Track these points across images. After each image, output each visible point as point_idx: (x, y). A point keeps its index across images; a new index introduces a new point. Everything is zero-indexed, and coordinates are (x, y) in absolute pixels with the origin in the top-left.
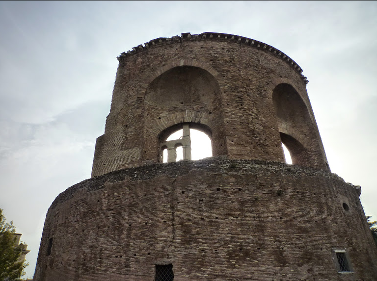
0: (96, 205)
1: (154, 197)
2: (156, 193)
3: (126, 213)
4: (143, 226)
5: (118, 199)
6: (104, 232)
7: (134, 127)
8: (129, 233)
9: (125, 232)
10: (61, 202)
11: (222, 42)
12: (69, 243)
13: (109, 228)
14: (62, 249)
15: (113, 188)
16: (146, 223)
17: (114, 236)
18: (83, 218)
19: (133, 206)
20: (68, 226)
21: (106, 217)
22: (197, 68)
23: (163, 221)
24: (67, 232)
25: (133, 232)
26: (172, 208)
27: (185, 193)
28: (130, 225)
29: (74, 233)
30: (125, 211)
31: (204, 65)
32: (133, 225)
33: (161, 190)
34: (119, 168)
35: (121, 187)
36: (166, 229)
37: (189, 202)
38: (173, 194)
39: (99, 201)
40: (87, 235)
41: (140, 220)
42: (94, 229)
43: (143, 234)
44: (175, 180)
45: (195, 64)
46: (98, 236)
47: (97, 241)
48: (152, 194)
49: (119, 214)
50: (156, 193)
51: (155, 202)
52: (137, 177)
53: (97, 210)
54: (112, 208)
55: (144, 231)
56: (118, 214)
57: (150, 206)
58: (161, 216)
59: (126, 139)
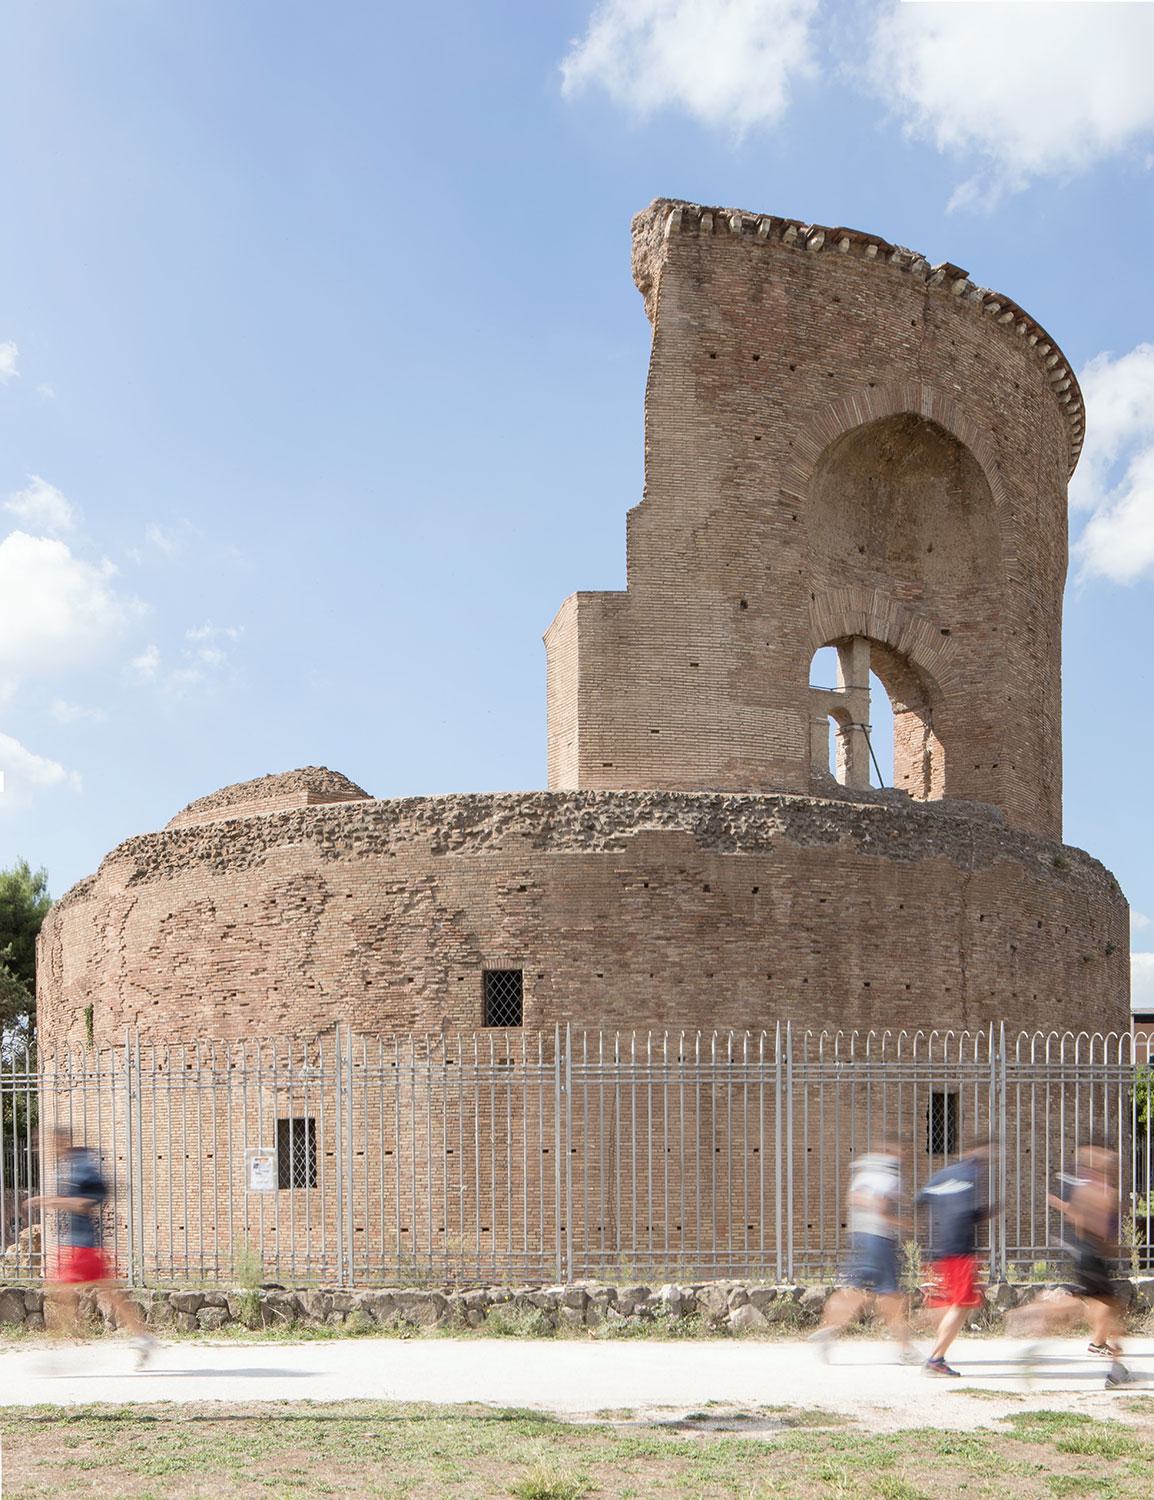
0: (750, 901)
1: (924, 919)
2: (928, 907)
3: (854, 948)
4: (900, 992)
5: (823, 901)
6: (791, 989)
7: (775, 622)
8: (866, 1009)
9: (856, 1002)
10: (535, 846)
11: (1016, 348)
12: (644, 1001)
13: (806, 981)
14: (604, 1018)
15: (804, 859)
16: (908, 987)
17: (826, 1007)
18: (700, 932)
19: (871, 930)
20: (621, 949)
21: (792, 947)
22: (960, 446)
23: (944, 986)
24: (624, 965)
25: (877, 1003)
26: (962, 956)
27: (985, 919)
28: (867, 984)
29: (666, 974)
30: (851, 941)
31: (982, 452)
32: (874, 984)
33: (941, 903)
34: (729, 766)
35: (829, 861)
36: (950, 1007)
37: (994, 946)
38: (962, 916)
39: (756, 890)
40: (728, 990)
41: (893, 974)
42: (756, 975)
43: (901, 1011)
44: (968, 880)
45: (961, 431)
46: (770, 1001)
47: (768, 1013)
48: (919, 908)
49: (835, 946)
50: (928, 907)
51: (927, 933)
52: (872, 843)
53: (757, 918)
54: (807, 922)
55: (905, 1007)
56: (829, 947)
57: (914, 940)
58: (940, 971)
59: (748, 661)
